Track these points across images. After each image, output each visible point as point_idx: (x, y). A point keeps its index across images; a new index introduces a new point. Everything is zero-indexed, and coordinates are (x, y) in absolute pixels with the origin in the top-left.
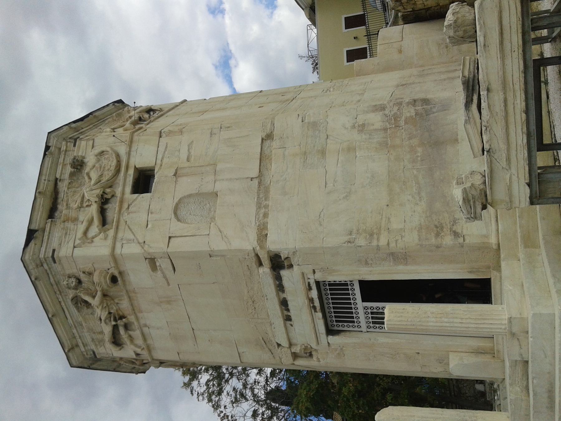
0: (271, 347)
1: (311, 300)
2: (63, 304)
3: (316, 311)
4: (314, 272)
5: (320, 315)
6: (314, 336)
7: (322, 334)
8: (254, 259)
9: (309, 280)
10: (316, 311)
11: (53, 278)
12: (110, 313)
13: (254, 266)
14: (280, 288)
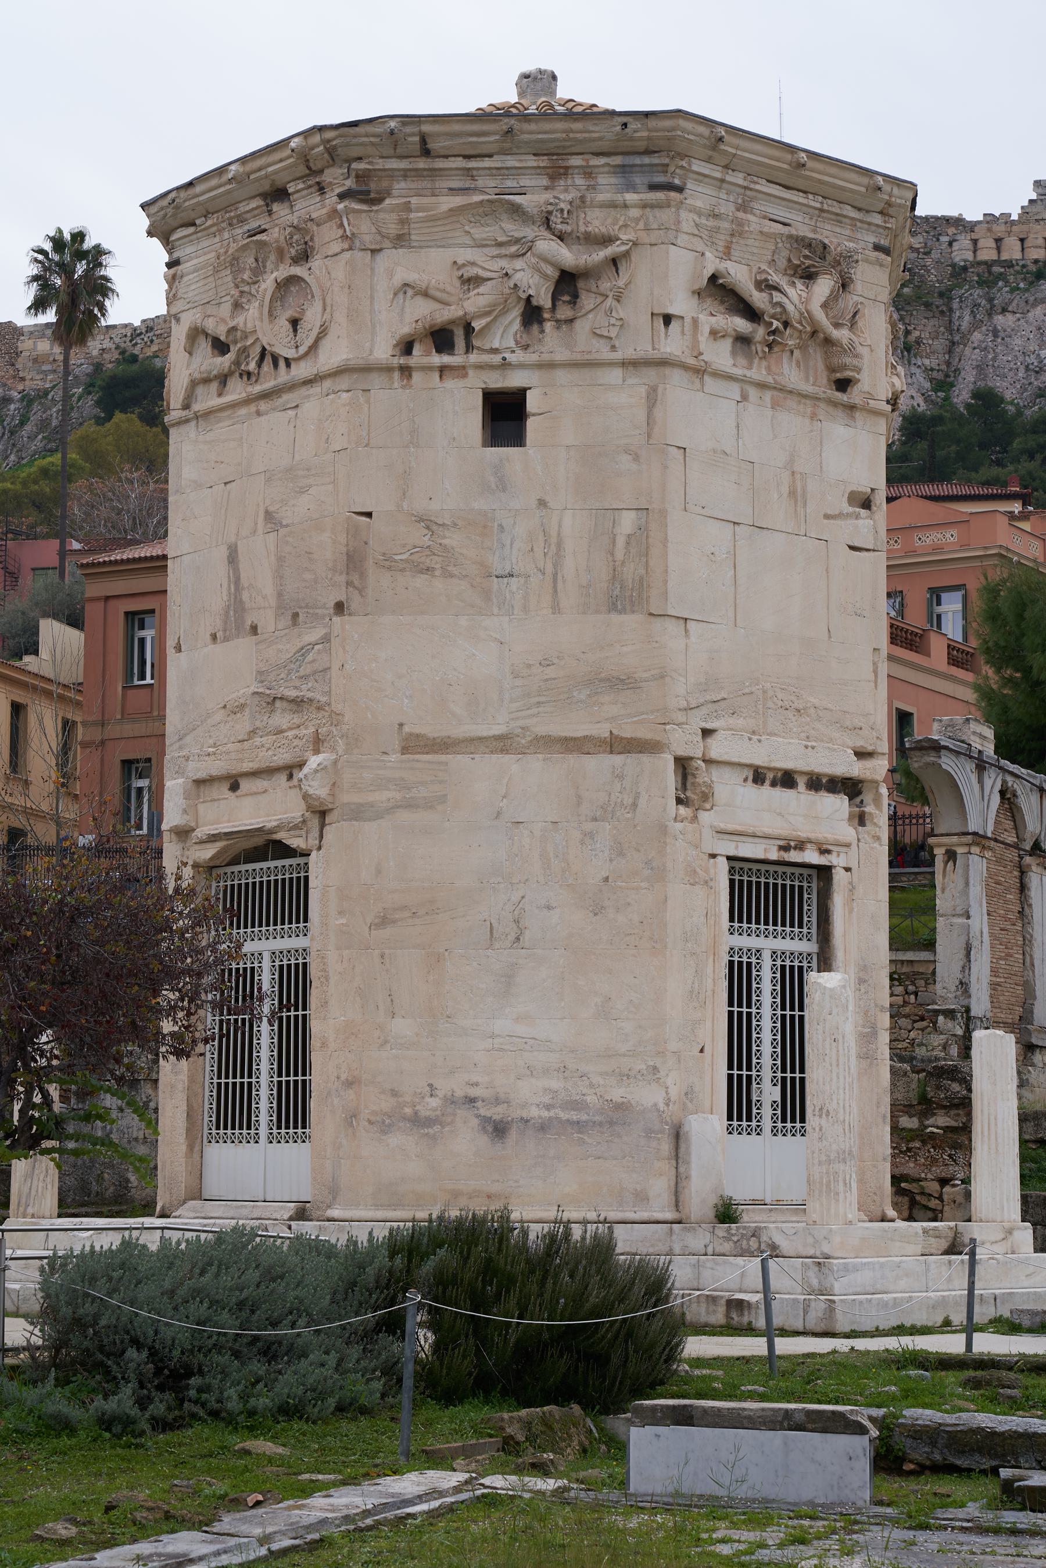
0: (704, 710)
1: (801, 846)
2: (799, 198)
3: (782, 848)
4: (848, 869)
5: (774, 855)
6: (739, 828)
7: (737, 847)
8: (870, 748)
9: (835, 854)
10: (782, 848)
11: (853, 219)
12: (786, 324)
13: (860, 743)
14: (817, 783)
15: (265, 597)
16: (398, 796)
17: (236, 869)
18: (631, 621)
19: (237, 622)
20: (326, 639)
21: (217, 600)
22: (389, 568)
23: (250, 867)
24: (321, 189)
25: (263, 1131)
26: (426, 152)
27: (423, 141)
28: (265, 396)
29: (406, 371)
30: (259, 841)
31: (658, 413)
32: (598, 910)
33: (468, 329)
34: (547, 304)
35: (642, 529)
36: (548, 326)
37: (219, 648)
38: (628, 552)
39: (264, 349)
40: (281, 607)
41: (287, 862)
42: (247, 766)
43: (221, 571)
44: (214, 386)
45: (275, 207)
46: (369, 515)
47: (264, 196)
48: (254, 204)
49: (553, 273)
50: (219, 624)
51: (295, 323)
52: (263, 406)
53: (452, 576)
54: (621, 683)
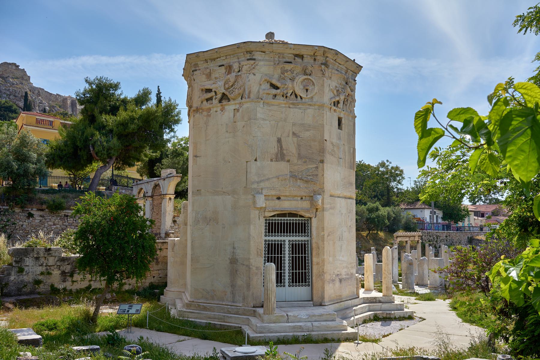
15: (293, 153)
17: (274, 218)
20: (317, 168)
23: (280, 218)
24: (315, 60)
25: (287, 284)
28: (292, 104)
37: (273, 163)
40: (300, 157)
42: (288, 194)
43: (275, 144)
44: (271, 96)
45: (296, 58)
47: (293, 54)
48: (291, 55)
50: (274, 157)
51: (307, 90)
52: (291, 106)
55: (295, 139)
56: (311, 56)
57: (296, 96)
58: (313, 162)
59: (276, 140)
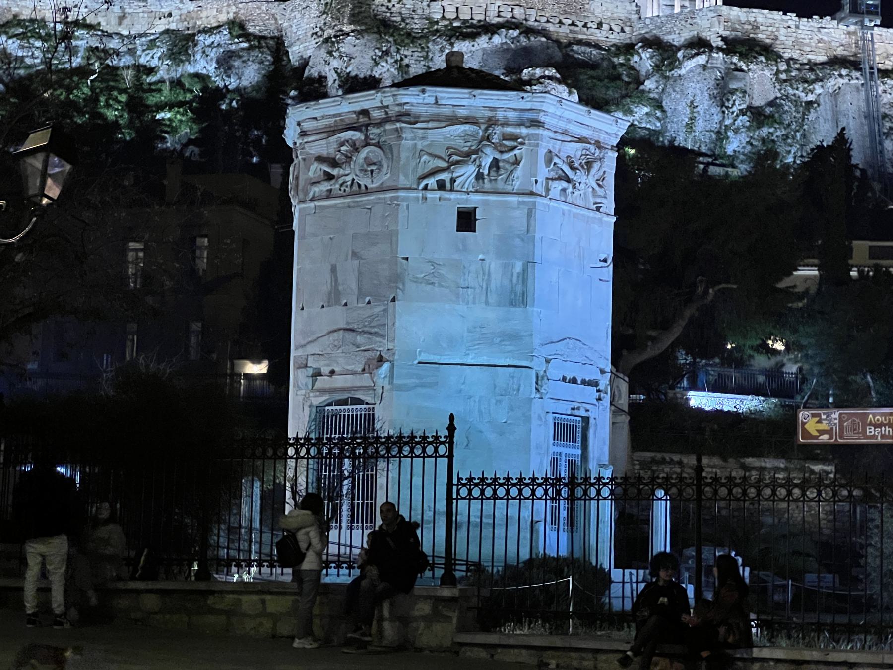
1: (578, 409)
16: (417, 381)
17: (330, 408)
18: (518, 311)
19: (334, 297)
20: (385, 310)
21: (326, 288)
22: (415, 282)
23: (338, 408)
26: (436, 103)
27: (436, 98)
29: (425, 198)
30: (345, 395)
31: (532, 222)
32: (502, 434)
33: (453, 180)
34: (486, 172)
35: (525, 270)
36: (486, 181)
38: (518, 280)
39: (353, 180)
40: (361, 295)
41: (359, 407)
43: (328, 276)
46: (407, 259)
47: (355, 112)
49: (490, 160)
51: (372, 171)
53: (442, 286)
54: (513, 337)
55: (356, 262)
56: (379, 108)
57: (359, 185)
58: (380, 301)
59: (330, 268)
